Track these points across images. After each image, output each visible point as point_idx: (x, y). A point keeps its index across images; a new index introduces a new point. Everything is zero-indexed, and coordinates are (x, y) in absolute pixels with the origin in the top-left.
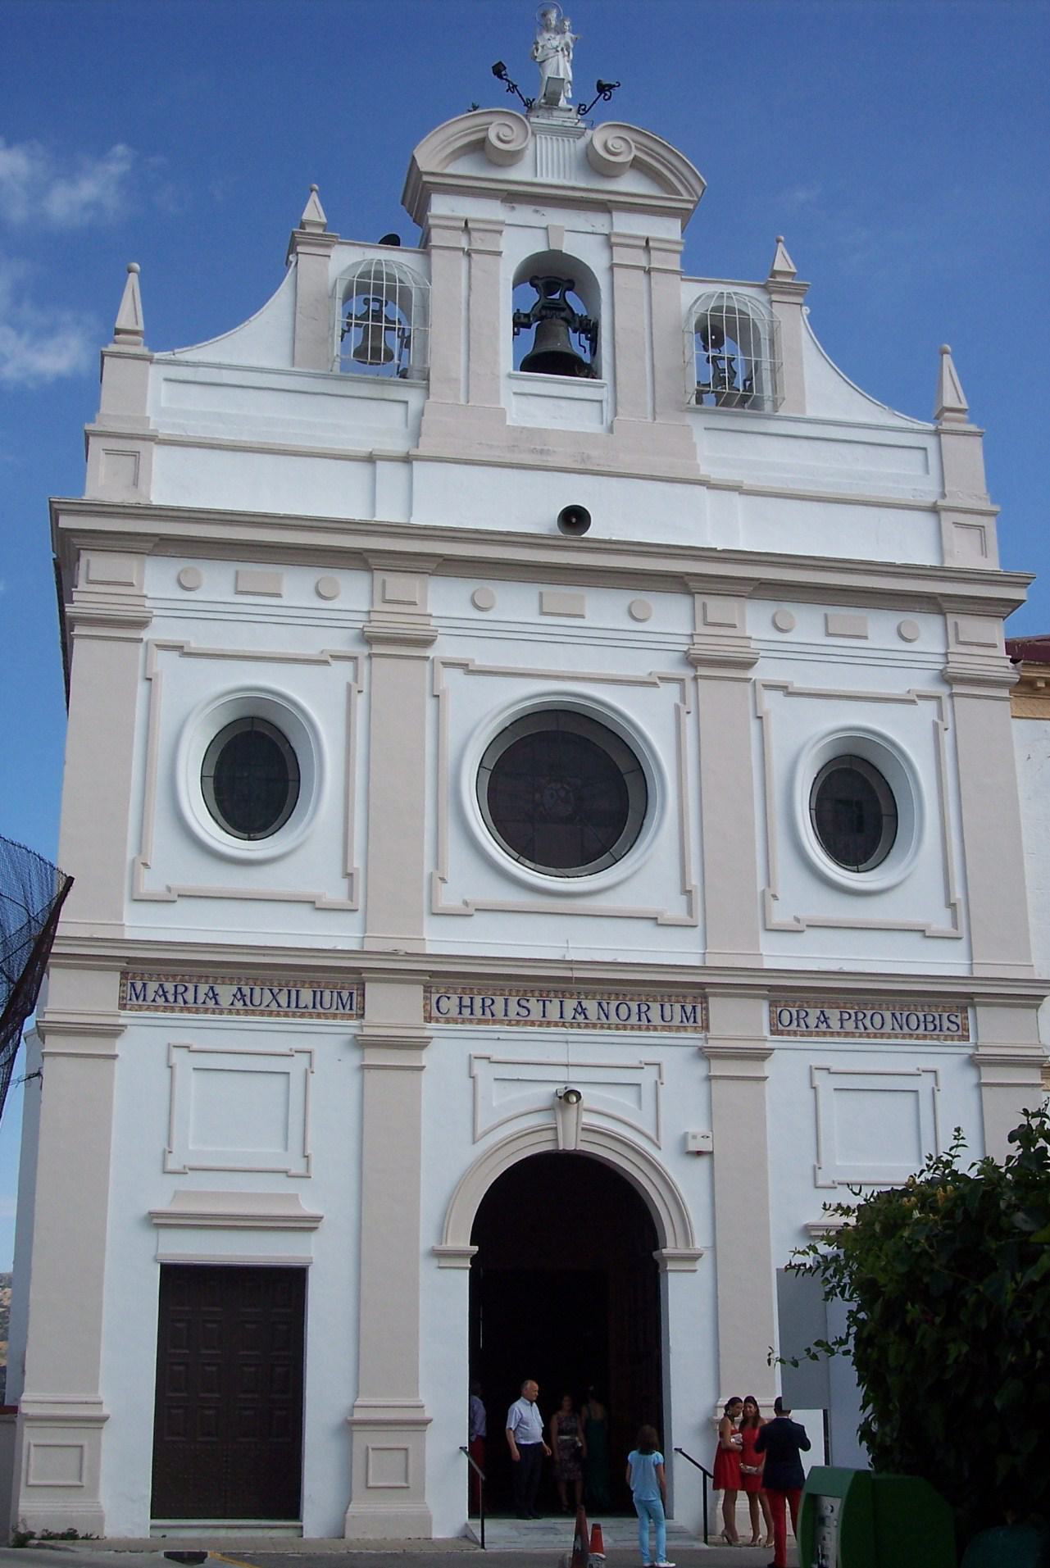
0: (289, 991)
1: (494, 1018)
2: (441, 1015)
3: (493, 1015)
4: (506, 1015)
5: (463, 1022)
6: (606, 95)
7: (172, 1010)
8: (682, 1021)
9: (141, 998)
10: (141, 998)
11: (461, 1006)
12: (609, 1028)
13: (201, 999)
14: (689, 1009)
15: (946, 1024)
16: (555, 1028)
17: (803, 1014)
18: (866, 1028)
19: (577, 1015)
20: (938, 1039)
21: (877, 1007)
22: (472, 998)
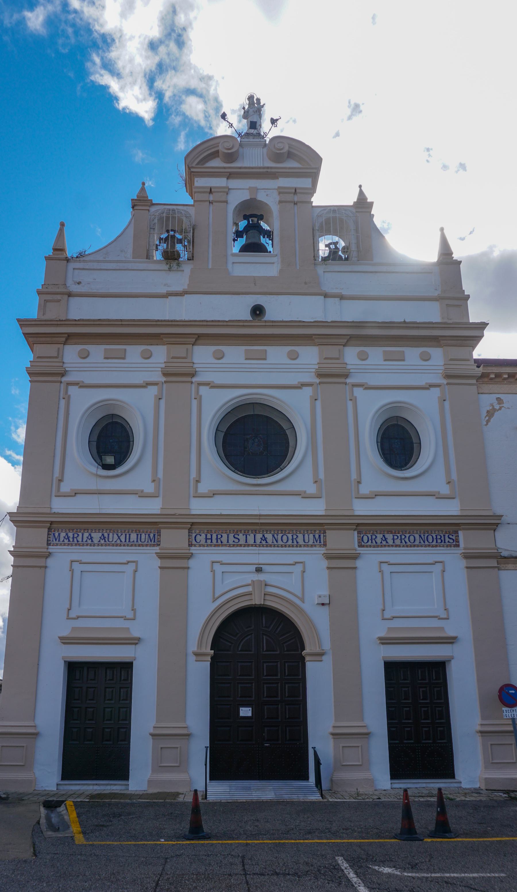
0: (126, 535)
1: (222, 544)
2: (197, 543)
3: (222, 542)
4: (228, 542)
5: (207, 546)
6: (275, 124)
7: (72, 545)
8: (314, 542)
9: (58, 540)
10: (58, 540)
11: (206, 539)
12: (278, 547)
13: (85, 540)
14: (317, 536)
15: (447, 539)
16: (251, 547)
17: (374, 537)
18: (406, 543)
19: (262, 541)
20: (443, 546)
21: (411, 532)
22: (211, 535)
